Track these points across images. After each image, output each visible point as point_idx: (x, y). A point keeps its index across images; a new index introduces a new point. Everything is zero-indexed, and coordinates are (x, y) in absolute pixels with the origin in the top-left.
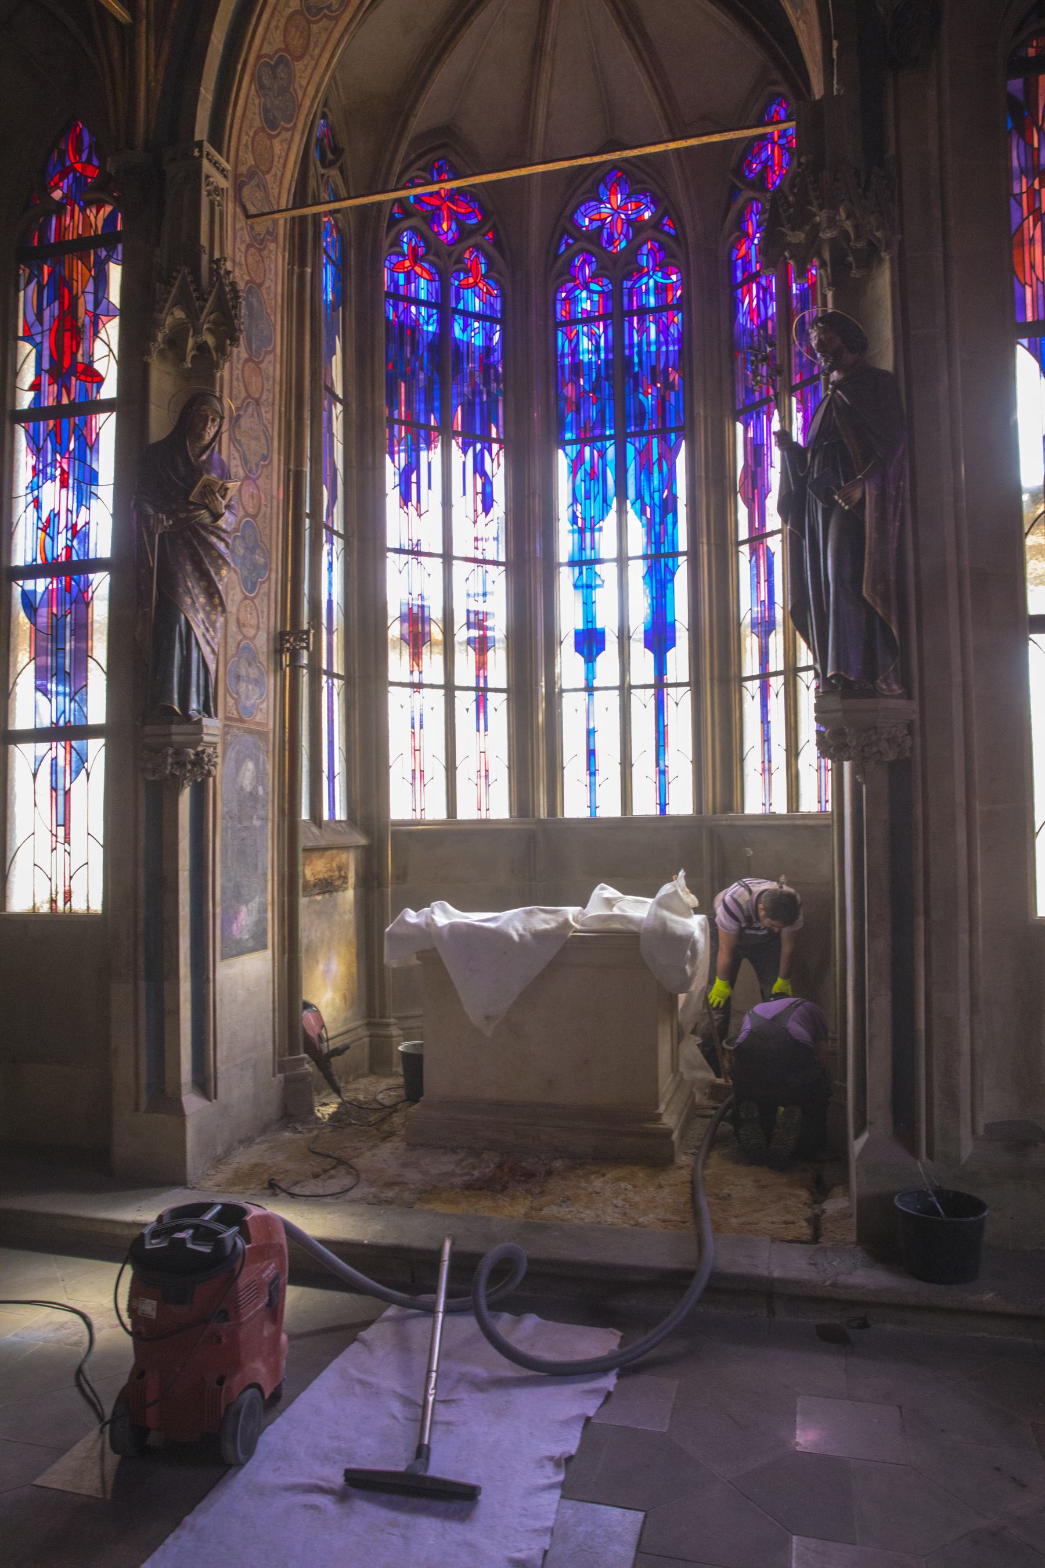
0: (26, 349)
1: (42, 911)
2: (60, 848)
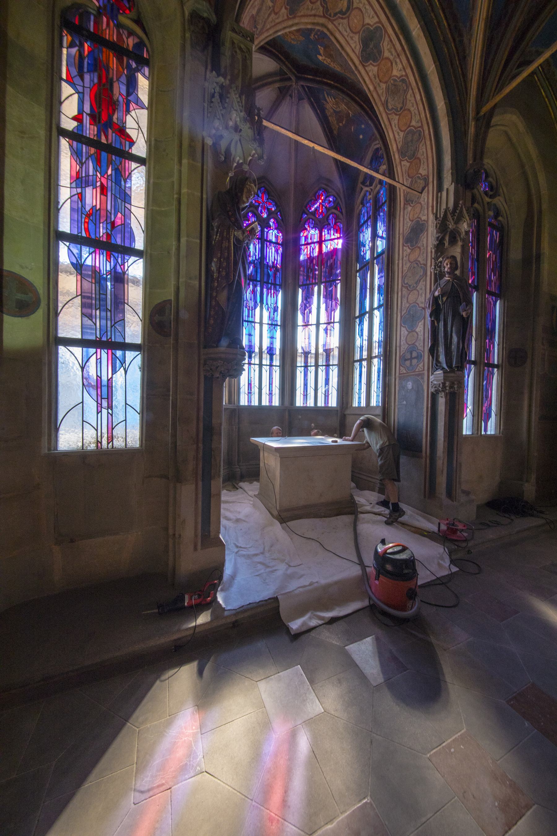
0: (66, 90)
1: (89, 448)
2: (104, 412)
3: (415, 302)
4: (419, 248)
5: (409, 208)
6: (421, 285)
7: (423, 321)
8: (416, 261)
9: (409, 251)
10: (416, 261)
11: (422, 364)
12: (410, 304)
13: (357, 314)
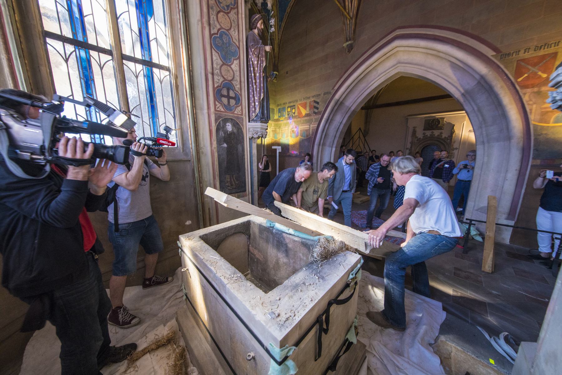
3: (228, 30)
11: (240, 107)
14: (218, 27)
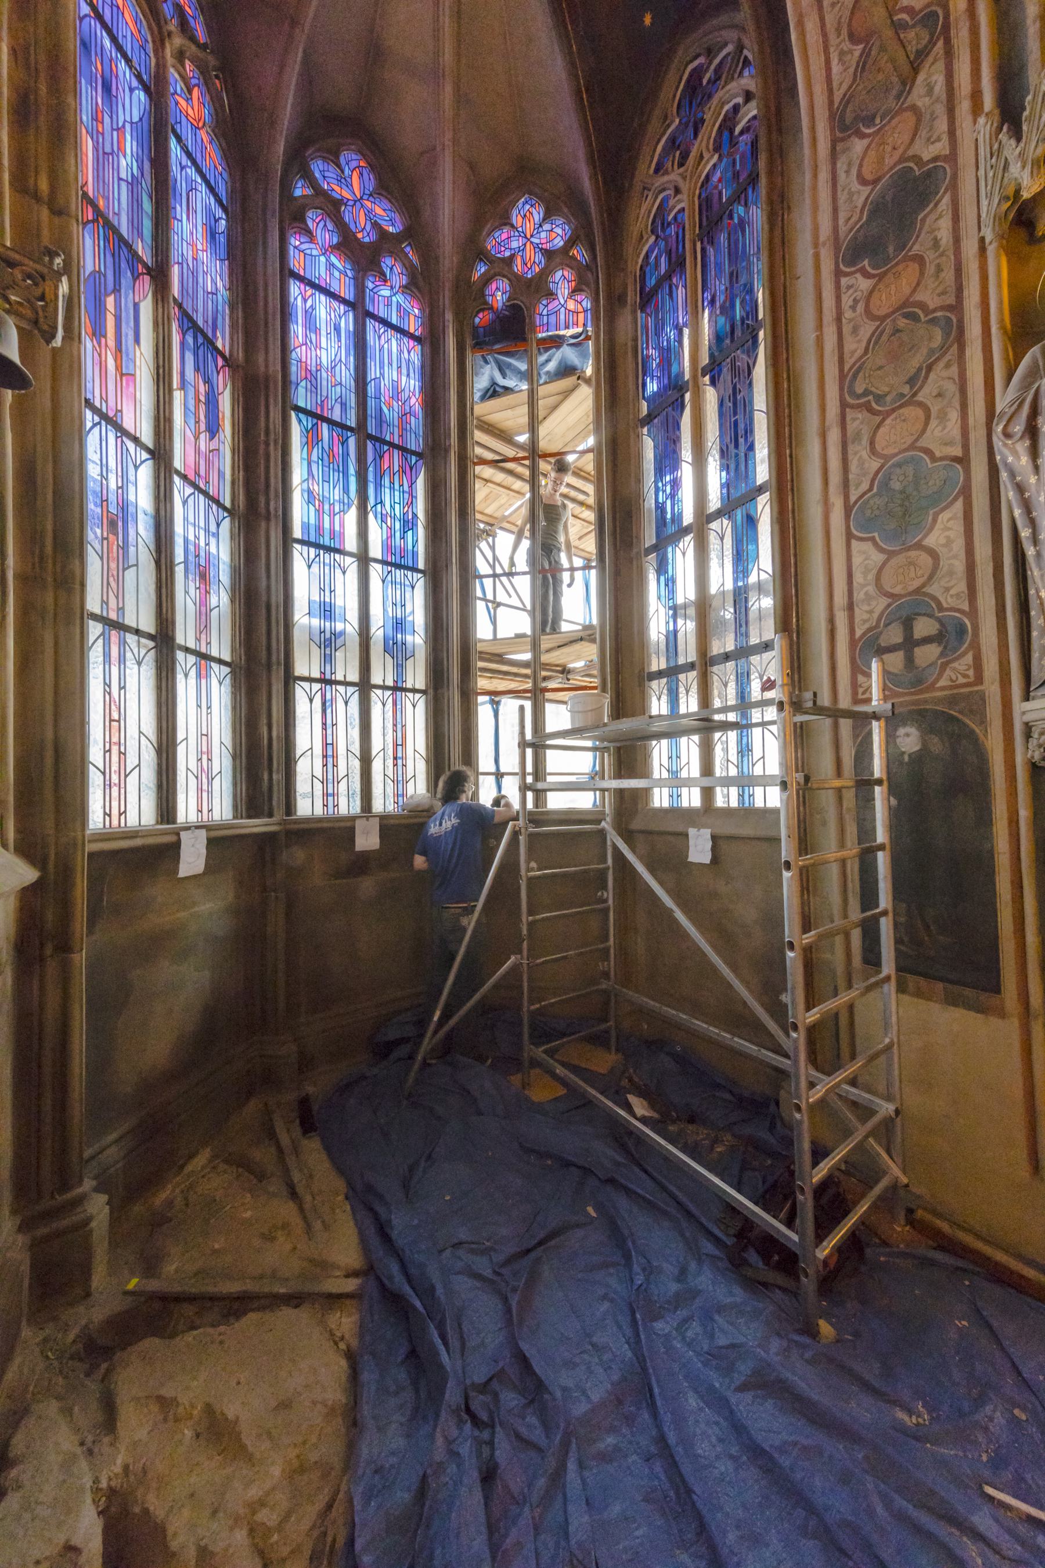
3: (912, 447)
4: (920, 260)
5: (858, 145)
6: (941, 378)
7: (959, 505)
8: (909, 310)
9: (864, 284)
10: (909, 310)
11: (969, 658)
12: (887, 458)
13: (649, 538)
14: (875, 465)
